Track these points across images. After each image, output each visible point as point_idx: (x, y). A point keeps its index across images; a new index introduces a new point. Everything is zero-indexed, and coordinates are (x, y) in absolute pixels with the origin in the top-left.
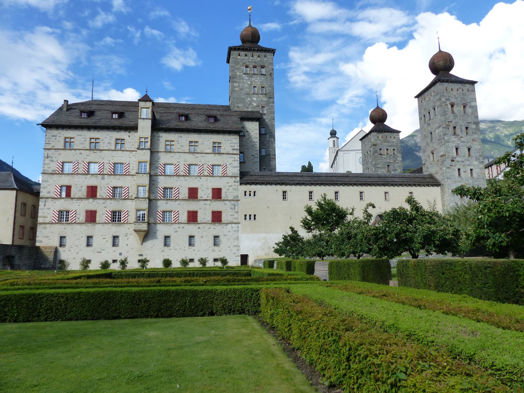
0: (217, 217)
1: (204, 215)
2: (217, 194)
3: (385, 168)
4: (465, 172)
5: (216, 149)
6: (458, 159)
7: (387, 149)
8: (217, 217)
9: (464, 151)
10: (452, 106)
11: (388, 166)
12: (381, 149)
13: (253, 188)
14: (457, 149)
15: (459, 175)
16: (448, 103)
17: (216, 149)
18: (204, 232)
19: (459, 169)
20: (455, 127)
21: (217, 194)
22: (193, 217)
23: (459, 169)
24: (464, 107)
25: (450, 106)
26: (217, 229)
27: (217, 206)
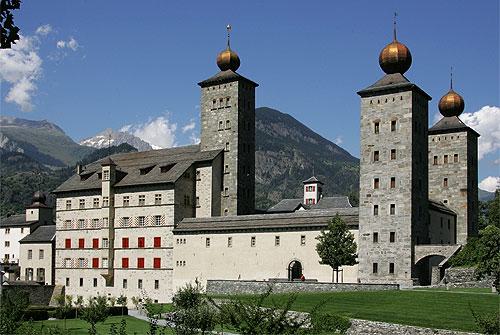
0: (157, 263)
1: (149, 263)
2: (157, 242)
3: (440, 183)
4: (382, 209)
5: (158, 202)
6: (377, 193)
7: (446, 156)
8: (157, 263)
9: (385, 181)
10: (377, 124)
11: (446, 180)
12: (436, 157)
13: (183, 237)
14: (377, 181)
15: (376, 213)
16: (371, 121)
17: (158, 202)
18: (149, 276)
19: (376, 207)
20: (377, 153)
21: (157, 242)
22: (141, 263)
23: (376, 207)
24: (394, 123)
25: (373, 125)
26: (158, 274)
27: (158, 253)
